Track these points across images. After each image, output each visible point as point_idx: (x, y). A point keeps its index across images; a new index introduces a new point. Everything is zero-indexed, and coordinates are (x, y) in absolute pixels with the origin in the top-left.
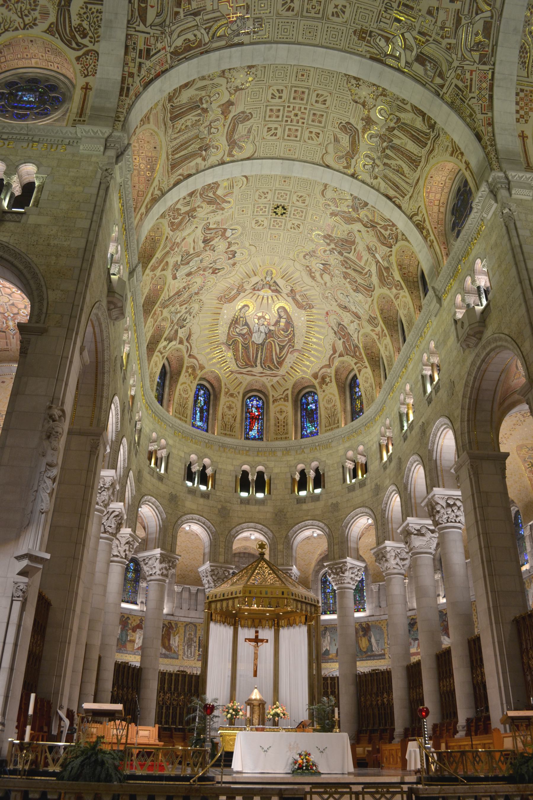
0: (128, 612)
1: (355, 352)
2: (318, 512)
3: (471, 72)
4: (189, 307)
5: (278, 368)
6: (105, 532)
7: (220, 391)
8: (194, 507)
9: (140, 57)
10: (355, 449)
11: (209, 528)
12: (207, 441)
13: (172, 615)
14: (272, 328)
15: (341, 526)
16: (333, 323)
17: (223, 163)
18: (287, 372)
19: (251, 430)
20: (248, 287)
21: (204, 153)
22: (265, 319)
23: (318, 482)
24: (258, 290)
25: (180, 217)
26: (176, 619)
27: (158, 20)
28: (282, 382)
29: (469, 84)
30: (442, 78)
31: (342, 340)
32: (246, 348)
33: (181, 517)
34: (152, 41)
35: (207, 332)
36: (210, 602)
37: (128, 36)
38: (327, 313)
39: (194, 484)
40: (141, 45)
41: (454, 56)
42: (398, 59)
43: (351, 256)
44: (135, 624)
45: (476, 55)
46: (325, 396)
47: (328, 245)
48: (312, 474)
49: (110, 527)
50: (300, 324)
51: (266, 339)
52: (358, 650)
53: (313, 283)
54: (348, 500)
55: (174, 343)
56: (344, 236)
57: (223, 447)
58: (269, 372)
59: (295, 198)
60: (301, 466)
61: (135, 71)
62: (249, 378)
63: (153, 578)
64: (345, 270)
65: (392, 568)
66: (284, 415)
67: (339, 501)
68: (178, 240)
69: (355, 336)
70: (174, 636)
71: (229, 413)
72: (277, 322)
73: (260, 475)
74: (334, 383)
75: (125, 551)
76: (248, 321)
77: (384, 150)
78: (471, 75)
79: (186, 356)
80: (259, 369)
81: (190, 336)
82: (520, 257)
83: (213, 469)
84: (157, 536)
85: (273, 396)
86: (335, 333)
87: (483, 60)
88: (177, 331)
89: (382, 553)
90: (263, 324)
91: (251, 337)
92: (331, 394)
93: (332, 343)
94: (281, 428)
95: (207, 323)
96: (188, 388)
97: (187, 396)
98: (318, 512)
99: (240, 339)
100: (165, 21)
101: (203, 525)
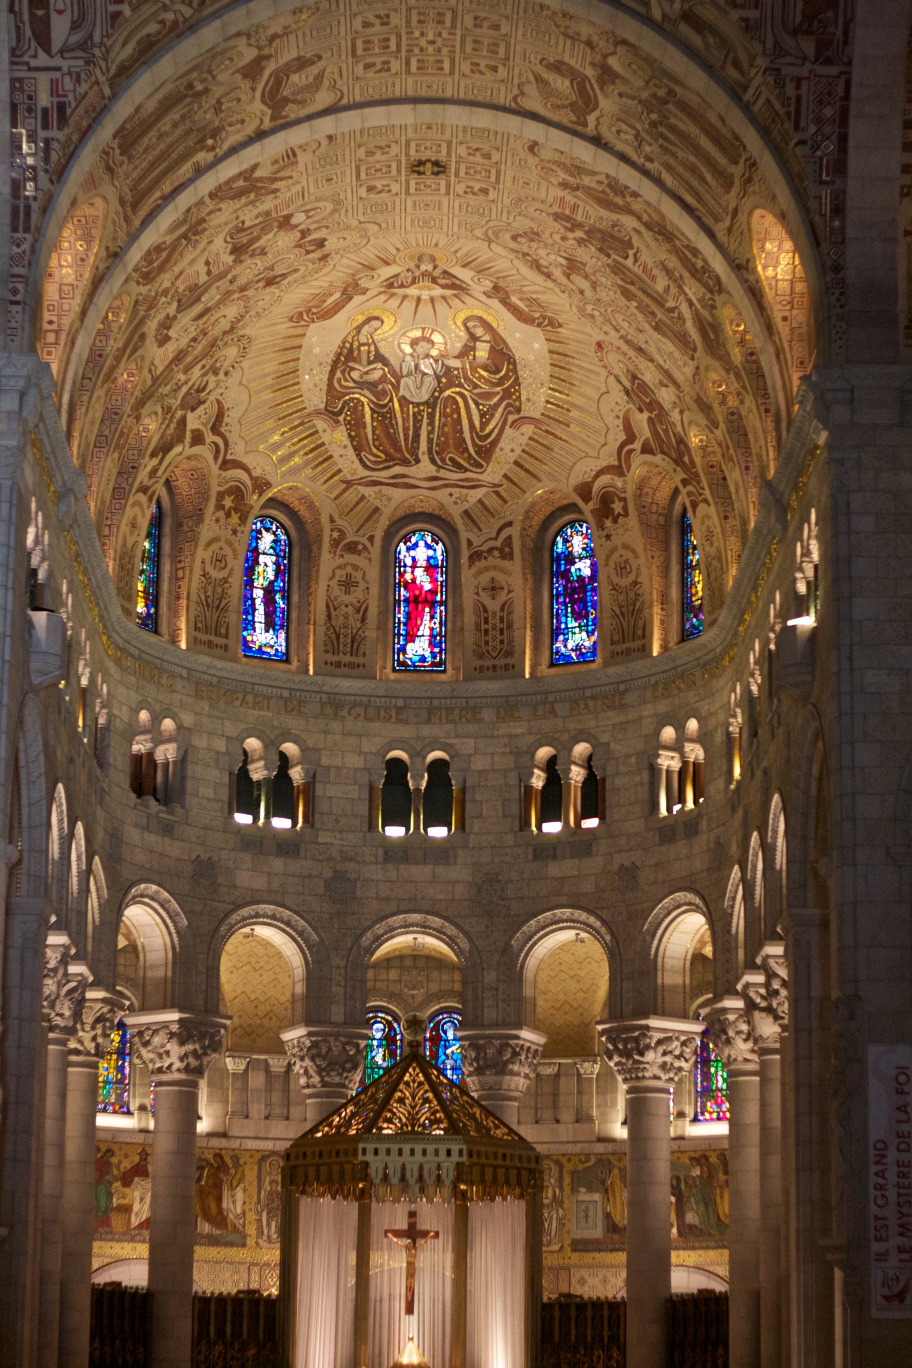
0: (110, 1136)
1: (681, 455)
2: (588, 886)
3: (798, 81)
4: (211, 361)
5: (481, 466)
6: (52, 1029)
7: (320, 536)
8: (259, 883)
9: (46, 126)
11: (301, 934)
12: (286, 694)
13: (224, 1135)
14: (455, 363)
15: (641, 931)
16: (619, 369)
17: (260, 135)
18: (505, 476)
19: (411, 637)
21: (210, 142)
22: (433, 343)
24: (402, 286)
25: (164, 254)
26: (235, 1144)
27: (75, 38)
28: (493, 502)
29: (792, 109)
30: (742, 72)
31: (646, 415)
32: (383, 415)
33: (228, 915)
34: (68, 84)
35: (268, 396)
36: (295, 1167)
37: (16, 84)
38: (599, 345)
39: (256, 819)
41: (757, 47)
43: (629, 262)
44: (127, 1165)
45: (809, 46)
46: (613, 550)
47: (572, 230)
48: (577, 774)
49: (61, 1015)
50: (531, 357)
52: (713, 1219)
53: (550, 284)
54: (656, 865)
55: (177, 449)
56: (603, 225)
58: (455, 476)
59: (462, 151)
60: (544, 752)
62: (398, 494)
63: (165, 1078)
64: (620, 282)
65: (740, 1059)
66: (502, 597)
67: (638, 863)
68: (166, 284)
69: (675, 416)
70: (232, 1188)
71: (347, 599)
72: (467, 351)
74: (633, 520)
75: (94, 1039)
76: (382, 351)
77: (653, 124)
78: (798, 87)
79: (215, 469)
80: (425, 468)
81: (220, 416)
83: (306, 772)
84: (169, 973)
85: (470, 543)
86: (627, 393)
88: (183, 422)
89: (719, 1020)
90: (427, 356)
91: (396, 388)
92: (626, 547)
93: (621, 415)
95: (266, 376)
96: (228, 551)
97: (224, 573)
98: (588, 886)
99: (364, 398)
100: (91, 36)
101: (286, 926)
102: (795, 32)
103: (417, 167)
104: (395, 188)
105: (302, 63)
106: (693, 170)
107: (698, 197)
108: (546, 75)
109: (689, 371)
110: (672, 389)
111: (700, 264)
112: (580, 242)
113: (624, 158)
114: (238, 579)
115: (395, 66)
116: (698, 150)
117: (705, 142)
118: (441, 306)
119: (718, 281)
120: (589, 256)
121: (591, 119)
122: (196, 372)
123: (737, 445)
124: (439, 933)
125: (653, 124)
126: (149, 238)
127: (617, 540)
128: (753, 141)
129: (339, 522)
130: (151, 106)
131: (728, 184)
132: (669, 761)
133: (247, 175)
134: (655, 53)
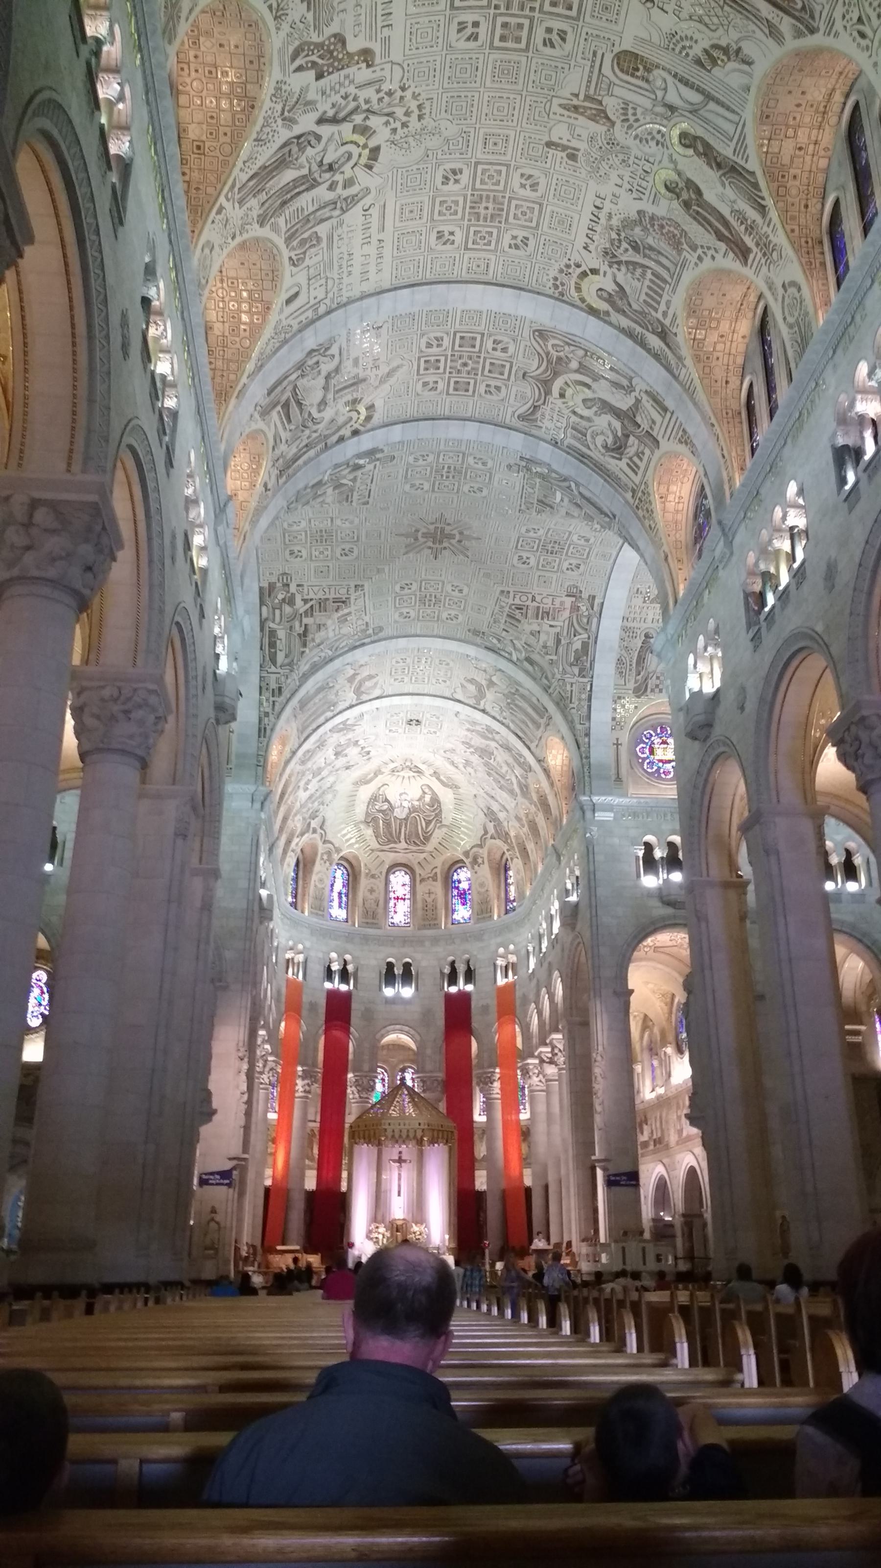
10: (506, 948)
17: (351, 707)
20: (386, 770)
23: (470, 976)
27: (287, 661)
28: (430, 858)
32: (387, 824)
34: (283, 679)
40: (273, 685)
42: (510, 654)
43: (492, 761)
45: (576, 670)
48: (461, 969)
51: (410, 813)
56: (483, 746)
57: (366, 939)
59: (428, 716)
60: (451, 958)
61: (269, 710)
62: (392, 855)
66: (433, 896)
69: (505, 824)
73: (407, 966)
77: (508, 704)
82: (592, 884)
87: (581, 674)
88: (309, 824)
94: (430, 913)
102: (571, 665)
103: (410, 722)
104: (400, 730)
105: (370, 677)
106: (524, 722)
107: (525, 733)
108: (466, 684)
109: (513, 805)
110: (505, 813)
111: (522, 760)
112: (472, 753)
113: (494, 718)
114: (328, 888)
115: (406, 679)
116: (527, 714)
117: (530, 710)
118: (412, 780)
119: (530, 767)
120: (475, 759)
121: (482, 702)
122: (316, 804)
123: (533, 834)
124: (407, 1033)
125: (508, 704)
126: (306, 746)
127: (479, 873)
128: (552, 708)
129: (369, 866)
130: (312, 692)
131: (538, 726)
132: (500, 962)
133: (344, 723)
134: (513, 675)
